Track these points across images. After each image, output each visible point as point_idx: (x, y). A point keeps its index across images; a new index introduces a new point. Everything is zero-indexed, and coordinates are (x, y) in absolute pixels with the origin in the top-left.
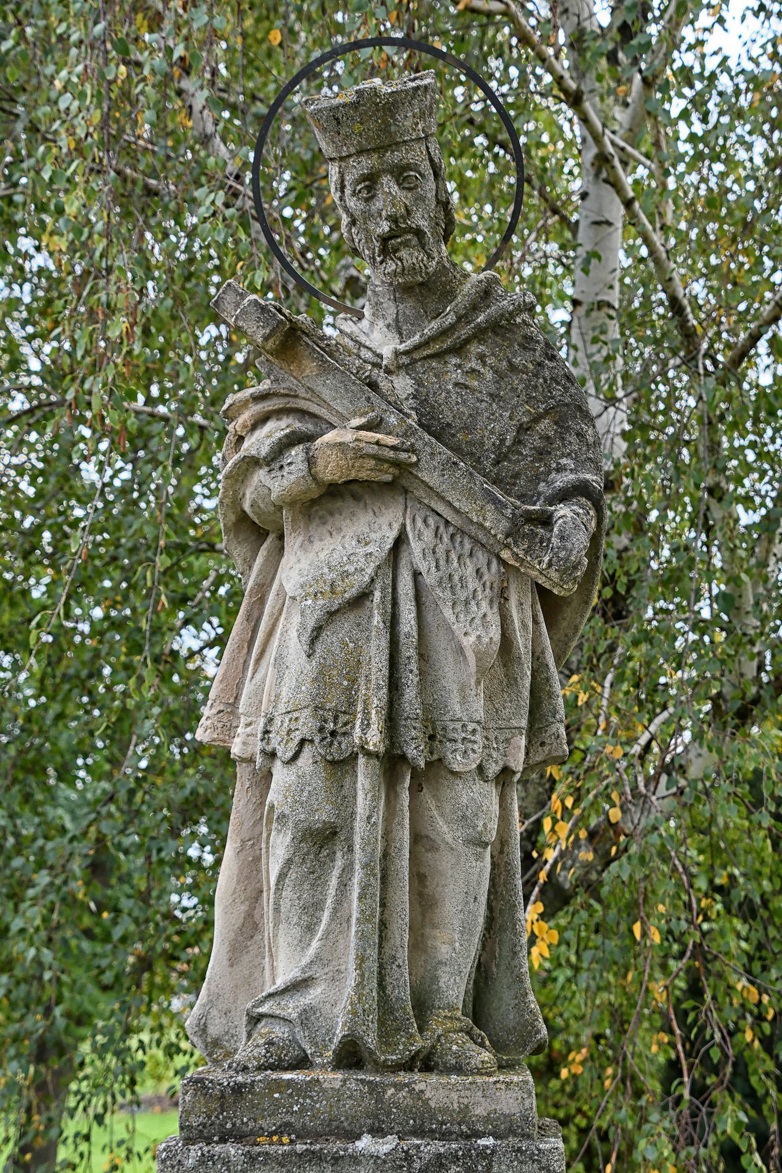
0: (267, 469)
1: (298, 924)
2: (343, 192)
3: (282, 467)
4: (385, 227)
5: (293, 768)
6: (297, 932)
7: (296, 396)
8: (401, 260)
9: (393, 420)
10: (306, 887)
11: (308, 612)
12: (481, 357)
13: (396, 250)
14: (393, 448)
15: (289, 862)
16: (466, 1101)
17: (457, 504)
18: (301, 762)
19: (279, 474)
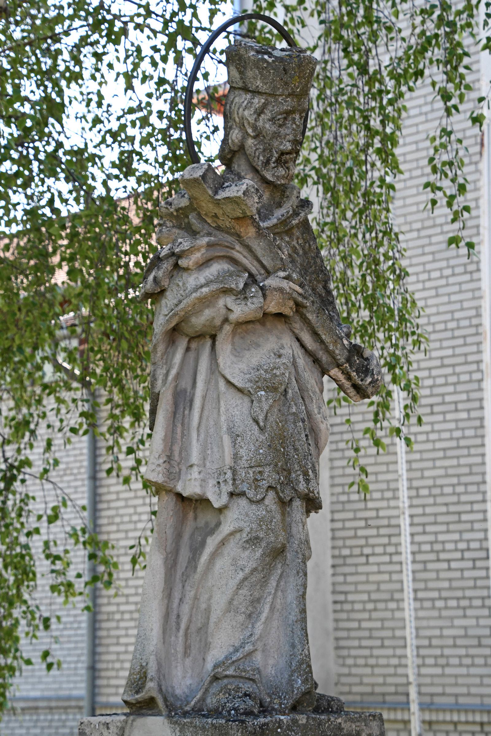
0: (234, 297)
1: (244, 613)
2: (259, 115)
3: (246, 298)
4: (288, 146)
5: (262, 507)
6: (241, 618)
7: (233, 249)
8: (288, 168)
9: (295, 276)
10: (258, 587)
11: (263, 399)
12: (298, 239)
13: (286, 162)
14: (300, 294)
15: (255, 570)
16: (358, 729)
17: (323, 337)
18: (267, 502)
19: (243, 302)
